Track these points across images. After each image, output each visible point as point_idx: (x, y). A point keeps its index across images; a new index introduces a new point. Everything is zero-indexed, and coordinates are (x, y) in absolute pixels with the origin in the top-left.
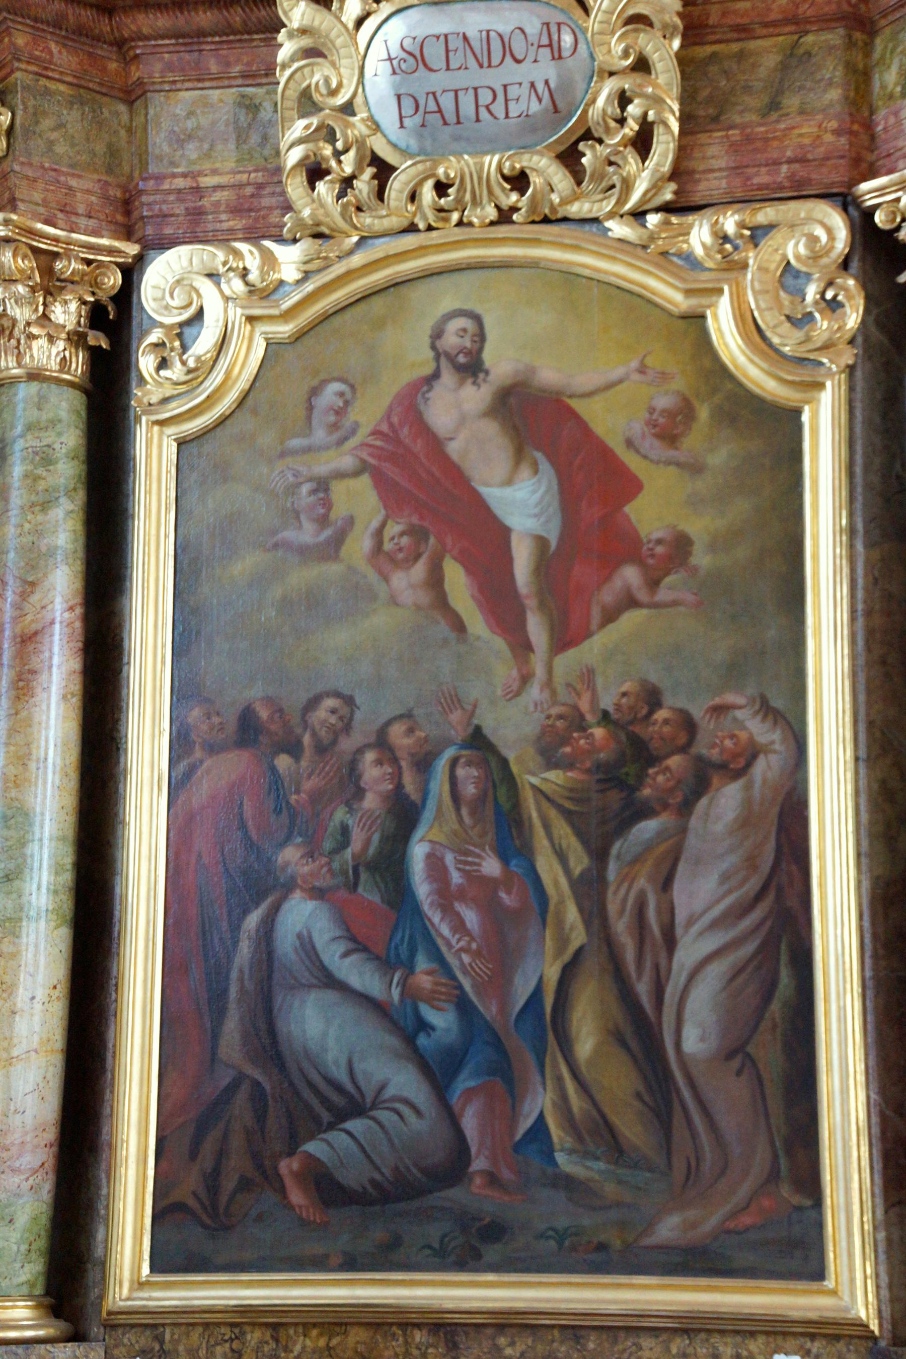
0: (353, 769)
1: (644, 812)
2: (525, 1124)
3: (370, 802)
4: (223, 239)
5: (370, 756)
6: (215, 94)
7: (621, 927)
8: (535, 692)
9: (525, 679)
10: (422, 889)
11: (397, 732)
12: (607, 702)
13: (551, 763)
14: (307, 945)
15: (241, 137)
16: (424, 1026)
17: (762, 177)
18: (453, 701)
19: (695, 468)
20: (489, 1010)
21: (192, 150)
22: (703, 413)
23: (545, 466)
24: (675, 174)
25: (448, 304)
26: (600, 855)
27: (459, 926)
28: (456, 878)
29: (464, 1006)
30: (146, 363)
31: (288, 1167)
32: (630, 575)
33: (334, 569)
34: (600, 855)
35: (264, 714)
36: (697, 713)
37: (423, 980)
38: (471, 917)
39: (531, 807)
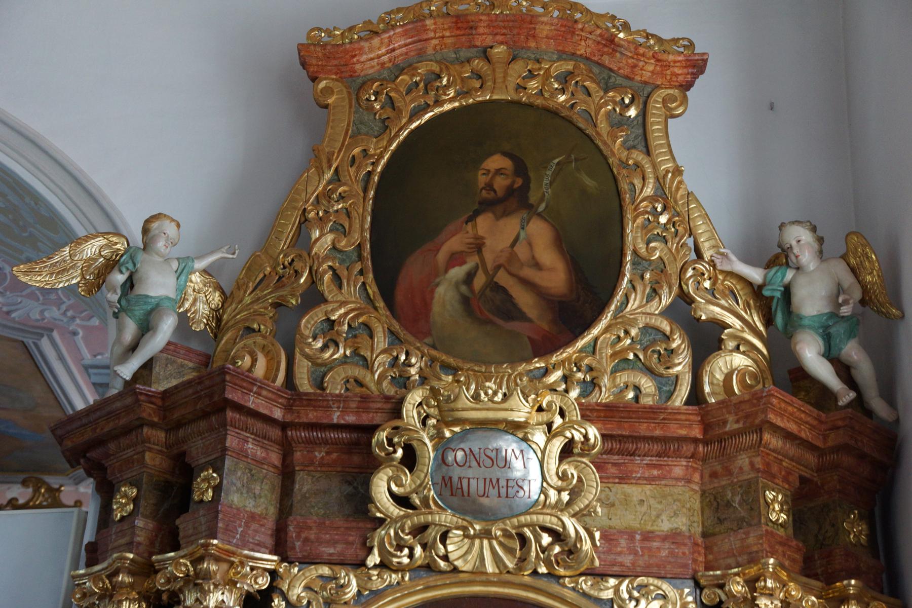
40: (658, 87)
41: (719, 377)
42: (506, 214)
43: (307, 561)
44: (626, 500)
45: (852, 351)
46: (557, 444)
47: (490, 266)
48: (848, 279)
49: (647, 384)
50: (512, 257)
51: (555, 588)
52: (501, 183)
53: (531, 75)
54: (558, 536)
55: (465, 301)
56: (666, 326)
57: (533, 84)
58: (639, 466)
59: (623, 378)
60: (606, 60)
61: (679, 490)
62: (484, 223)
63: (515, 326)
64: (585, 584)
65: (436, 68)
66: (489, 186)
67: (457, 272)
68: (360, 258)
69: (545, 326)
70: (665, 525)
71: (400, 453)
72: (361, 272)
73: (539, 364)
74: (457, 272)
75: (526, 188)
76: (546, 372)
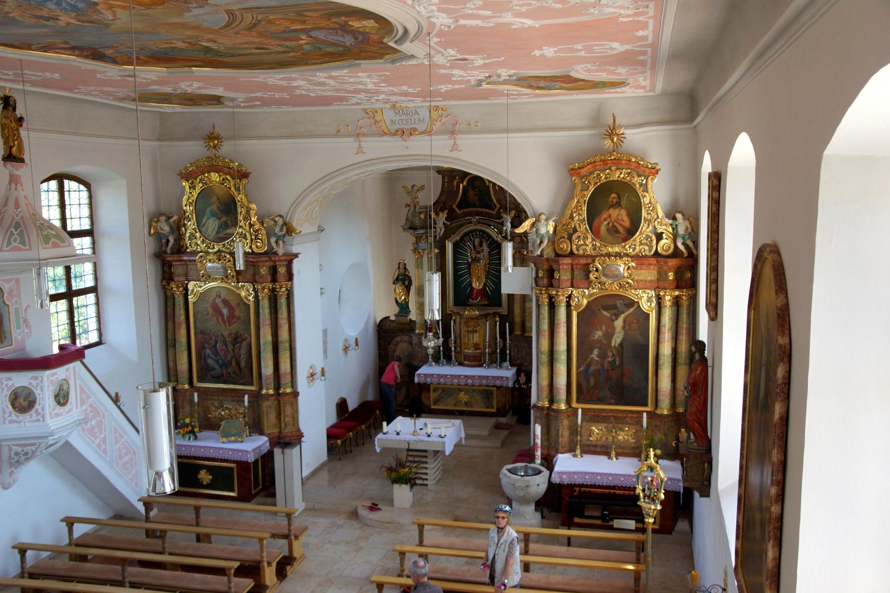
0: (211, 337)
1: (238, 343)
7: (236, 354)
10: (218, 349)
20: (225, 361)
22: (241, 304)
24: (237, 279)
32: (235, 320)
36: (242, 333)
37: (219, 357)
38: (223, 352)
41: (662, 245)
42: (616, 208)
44: (641, 274)
45: (689, 242)
47: (613, 221)
48: (689, 226)
49: (646, 248)
50: (618, 219)
51: (627, 292)
52: (615, 201)
53: (621, 174)
55: (608, 230)
56: (650, 234)
59: (641, 247)
61: (652, 271)
62: (611, 210)
63: (618, 235)
64: (633, 291)
67: (606, 223)
68: (584, 221)
69: (625, 235)
70: (649, 278)
73: (623, 244)
74: (606, 223)
75: (620, 201)
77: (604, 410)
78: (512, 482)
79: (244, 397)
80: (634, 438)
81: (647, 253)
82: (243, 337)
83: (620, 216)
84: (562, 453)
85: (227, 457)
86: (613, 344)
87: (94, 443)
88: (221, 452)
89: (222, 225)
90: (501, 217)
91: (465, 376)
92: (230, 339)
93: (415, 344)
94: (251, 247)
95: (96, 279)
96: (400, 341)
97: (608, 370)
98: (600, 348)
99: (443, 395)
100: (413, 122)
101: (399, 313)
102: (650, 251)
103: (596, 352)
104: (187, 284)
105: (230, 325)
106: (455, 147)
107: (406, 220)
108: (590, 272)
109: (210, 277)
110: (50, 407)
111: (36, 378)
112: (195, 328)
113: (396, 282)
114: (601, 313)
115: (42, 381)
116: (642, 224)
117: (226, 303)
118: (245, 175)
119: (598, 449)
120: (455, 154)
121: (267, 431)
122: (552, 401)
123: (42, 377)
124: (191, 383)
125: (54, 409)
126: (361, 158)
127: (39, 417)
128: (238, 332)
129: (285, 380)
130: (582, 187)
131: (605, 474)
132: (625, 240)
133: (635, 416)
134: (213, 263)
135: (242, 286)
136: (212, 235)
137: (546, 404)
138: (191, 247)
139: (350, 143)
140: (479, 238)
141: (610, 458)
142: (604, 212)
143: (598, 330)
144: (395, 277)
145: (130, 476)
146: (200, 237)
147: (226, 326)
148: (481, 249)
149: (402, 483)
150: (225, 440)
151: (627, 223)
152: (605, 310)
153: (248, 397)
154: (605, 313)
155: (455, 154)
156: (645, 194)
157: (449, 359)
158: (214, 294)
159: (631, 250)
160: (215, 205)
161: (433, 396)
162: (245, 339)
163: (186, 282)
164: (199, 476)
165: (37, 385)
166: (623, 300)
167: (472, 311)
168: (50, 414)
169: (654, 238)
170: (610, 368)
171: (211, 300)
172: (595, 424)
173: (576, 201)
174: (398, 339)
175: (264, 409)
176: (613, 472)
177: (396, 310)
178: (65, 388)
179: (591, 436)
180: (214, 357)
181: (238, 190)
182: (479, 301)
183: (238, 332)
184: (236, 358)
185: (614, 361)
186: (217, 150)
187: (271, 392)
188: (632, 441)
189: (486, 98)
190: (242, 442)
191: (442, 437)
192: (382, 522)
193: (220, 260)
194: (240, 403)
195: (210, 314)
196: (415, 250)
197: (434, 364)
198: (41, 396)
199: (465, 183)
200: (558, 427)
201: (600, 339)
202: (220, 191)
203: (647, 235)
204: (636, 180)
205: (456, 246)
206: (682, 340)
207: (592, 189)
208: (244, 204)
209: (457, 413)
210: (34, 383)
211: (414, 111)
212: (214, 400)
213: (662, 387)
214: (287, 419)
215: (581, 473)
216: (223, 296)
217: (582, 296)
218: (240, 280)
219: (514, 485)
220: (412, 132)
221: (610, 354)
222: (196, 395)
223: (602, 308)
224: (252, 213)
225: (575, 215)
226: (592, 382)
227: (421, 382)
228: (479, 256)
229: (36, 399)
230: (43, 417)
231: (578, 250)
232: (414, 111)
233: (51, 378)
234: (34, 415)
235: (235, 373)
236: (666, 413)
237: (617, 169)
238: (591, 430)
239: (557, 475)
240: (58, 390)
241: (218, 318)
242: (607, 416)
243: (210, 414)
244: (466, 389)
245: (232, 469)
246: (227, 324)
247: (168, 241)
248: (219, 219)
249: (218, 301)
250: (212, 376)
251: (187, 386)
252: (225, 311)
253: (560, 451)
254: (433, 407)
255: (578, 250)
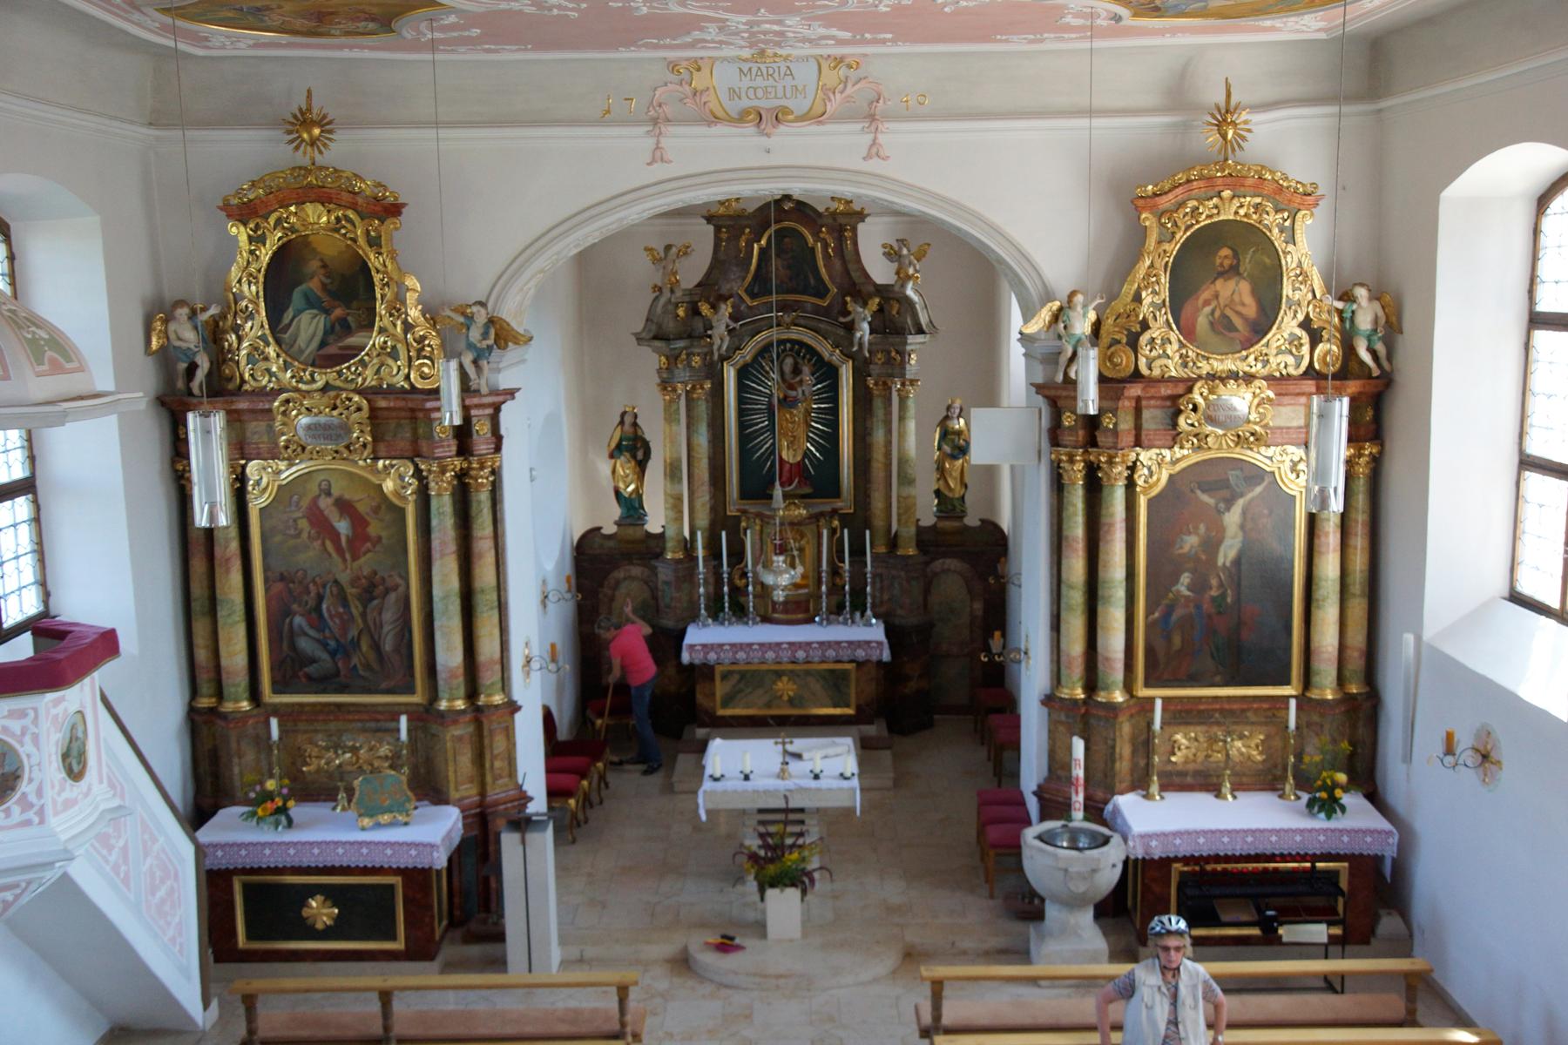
0: (308, 585)
1: (374, 598)
2: (353, 664)
3: (312, 594)
4: (265, 459)
5: (311, 585)
6: (262, 423)
7: (371, 624)
8: (348, 571)
9: (346, 568)
10: (326, 614)
11: (317, 579)
12: (365, 574)
13: (353, 587)
14: (300, 627)
15: (269, 433)
16: (328, 644)
17: (393, 453)
18: (329, 572)
19: (381, 520)
20: (343, 641)
21: (256, 437)
22: (383, 507)
23: (348, 519)
24: (374, 451)
25: (322, 478)
26: (365, 607)
27: (335, 622)
28: (333, 612)
29: (337, 640)
30: (250, 488)
31: (301, 674)
32: (369, 545)
33: (299, 541)
34: (365, 607)
35: (285, 574)
36: (386, 576)
38: (337, 621)
39: (349, 597)
40: (1299, 210)
42: (1229, 278)
43: (1150, 447)
45: (1380, 348)
46: (1256, 401)
47: (1222, 305)
48: (1381, 313)
49: (1290, 360)
50: (1232, 300)
52: (1227, 263)
53: (1242, 206)
54: (1252, 434)
55: (1212, 324)
57: (1242, 212)
58: (1286, 400)
59: (1280, 358)
60: (1277, 197)
62: (1219, 283)
63: (1232, 335)
65: (1194, 203)
66: (1221, 265)
67: (1208, 309)
68: (1164, 305)
69: (1246, 334)
70: (1295, 424)
71: (1191, 406)
72: (1165, 313)
73: (1244, 353)
74: (1208, 309)
76: (1247, 357)
77: (1200, 698)
78: (1062, 865)
79: (398, 721)
80: (1261, 753)
81: (1292, 371)
82: (389, 583)
83: (1238, 294)
84: (1122, 793)
85: (378, 861)
86: (1220, 562)
87: (107, 861)
88: (365, 851)
89: (333, 327)
90: (847, 313)
91: (791, 644)
92: (354, 591)
93: (666, 583)
94: (407, 377)
95: (32, 459)
96: (625, 579)
97: (1209, 616)
98: (1194, 571)
99: (742, 685)
100: (780, 94)
101: (622, 518)
102: (1298, 366)
103: (1185, 579)
104: (244, 467)
105: (355, 558)
106: (874, 151)
107: (647, 320)
108: (1180, 412)
109: (304, 449)
110: (53, 787)
111: (22, 714)
112: (266, 568)
113: (616, 453)
114: (1197, 498)
115: (36, 721)
116: (1282, 312)
117: (344, 506)
118: (395, 210)
119: (1189, 780)
120: (874, 166)
121: (454, 795)
122: (1091, 685)
123: (35, 710)
124: (255, 695)
125: (62, 789)
126: (659, 172)
127: (31, 814)
128: (375, 573)
129: (489, 677)
130: (1160, 234)
131: (1237, 832)
132: (1248, 344)
133: (1265, 706)
134: (316, 415)
135: (385, 466)
136: (307, 352)
137: (1079, 694)
138: (255, 379)
139: (636, 140)
140: (794, 358)
141: (1219, 795)
142: (1204, 287)
143: (1189, 533)
144: (613, 445)
145: (171, 933)
146: (278, 356)
147: (345, 560)
148: (798, 379)
149: (786, 886)
150: (366, 821)
151: (1251, 310)
152: (1203, 491)
153: (409, 720)
154: (1205, 498)
155: (874, 166)
156: (1290, 248)
157: (740, 613)
158: (313, 489)
159: (1260, 365)
160: (316, 280)
161: (720, 689)
162: (395, 588)
163: (243, 462)
164: (305, 912)
165: (24, 731)
166: (1242, 470)
167: (793, 507)
168: (54, 802)
169: (1306, 339)
170: (1213, 610)
171: (305, 503)
172: (1182, 728)
173: (1148, 263)
174: (619, 574)
175: (449, 745)
176: (1254, 826)
177: (616, 512)
178: (80, 734)
179: (1174, 754)
180: (312, 633)
181: (374, 243)
182: (796, 487)
183: (375, 573)
184: (369, 631)
185: (1223, 596)
186: (321, 152)
187: (460, 704)
188: (1259, 758)
189: (985, 39)
190: (406, 824)
191: (846, 778)
192: (765, 976)
193: (335, 408)
194: (379, 735)
195: (305, 535)
196: (666, 384)
197: (710, 621)
198: (35, 760)
199: (763, 242)
200: (1114, 740)
201: (1193, 551)
202: (330, 247)
203: (1291, 334)
204: (1272, 219)
205: (743, 374)
206: (1356, 548)
207: (1181, 237)
208: (391, 279)
209: (771, 722)
210: (15, 726)
211: (783, 69)
212: (316, 731)
213: (1324, 644)
214: (497, 764)
215: (1188, 833)
216: (336, 492)
217: (1159, 464)
218: (381, 454)
219: (1066, 871)
220: (779, 116)
221: (1214, 582)
222: (274, 722)
223: (1199, 488)
224: (411, 298)
225: (1144, 294)
226: (1177, 641)
227: (697, 662)
228: (793, 393)
229: (20, 767)
230: (41, 812)
231: (1150, 369)
232: (783, 69)
233: (54, 711)
234: (16, 810)
235: (368, 667)
236: (1330, 697)
237: (1233, 197)
238: (1175, 742)
239: (1137, 840)
240: (68, 740)
241: (323, 544)
242: (1207, 710)
243: (307, 764)
244: (792, 671)
245: (391, 887)
246: (348, 556)
247: (192, 368)
248: (327, 312)
249: (325, 503)
250: (309, 678)
251: (245, 705)
252: (343, 527)
253: (1116, 791)
254: (721, 712)
255: (1150, 369)
